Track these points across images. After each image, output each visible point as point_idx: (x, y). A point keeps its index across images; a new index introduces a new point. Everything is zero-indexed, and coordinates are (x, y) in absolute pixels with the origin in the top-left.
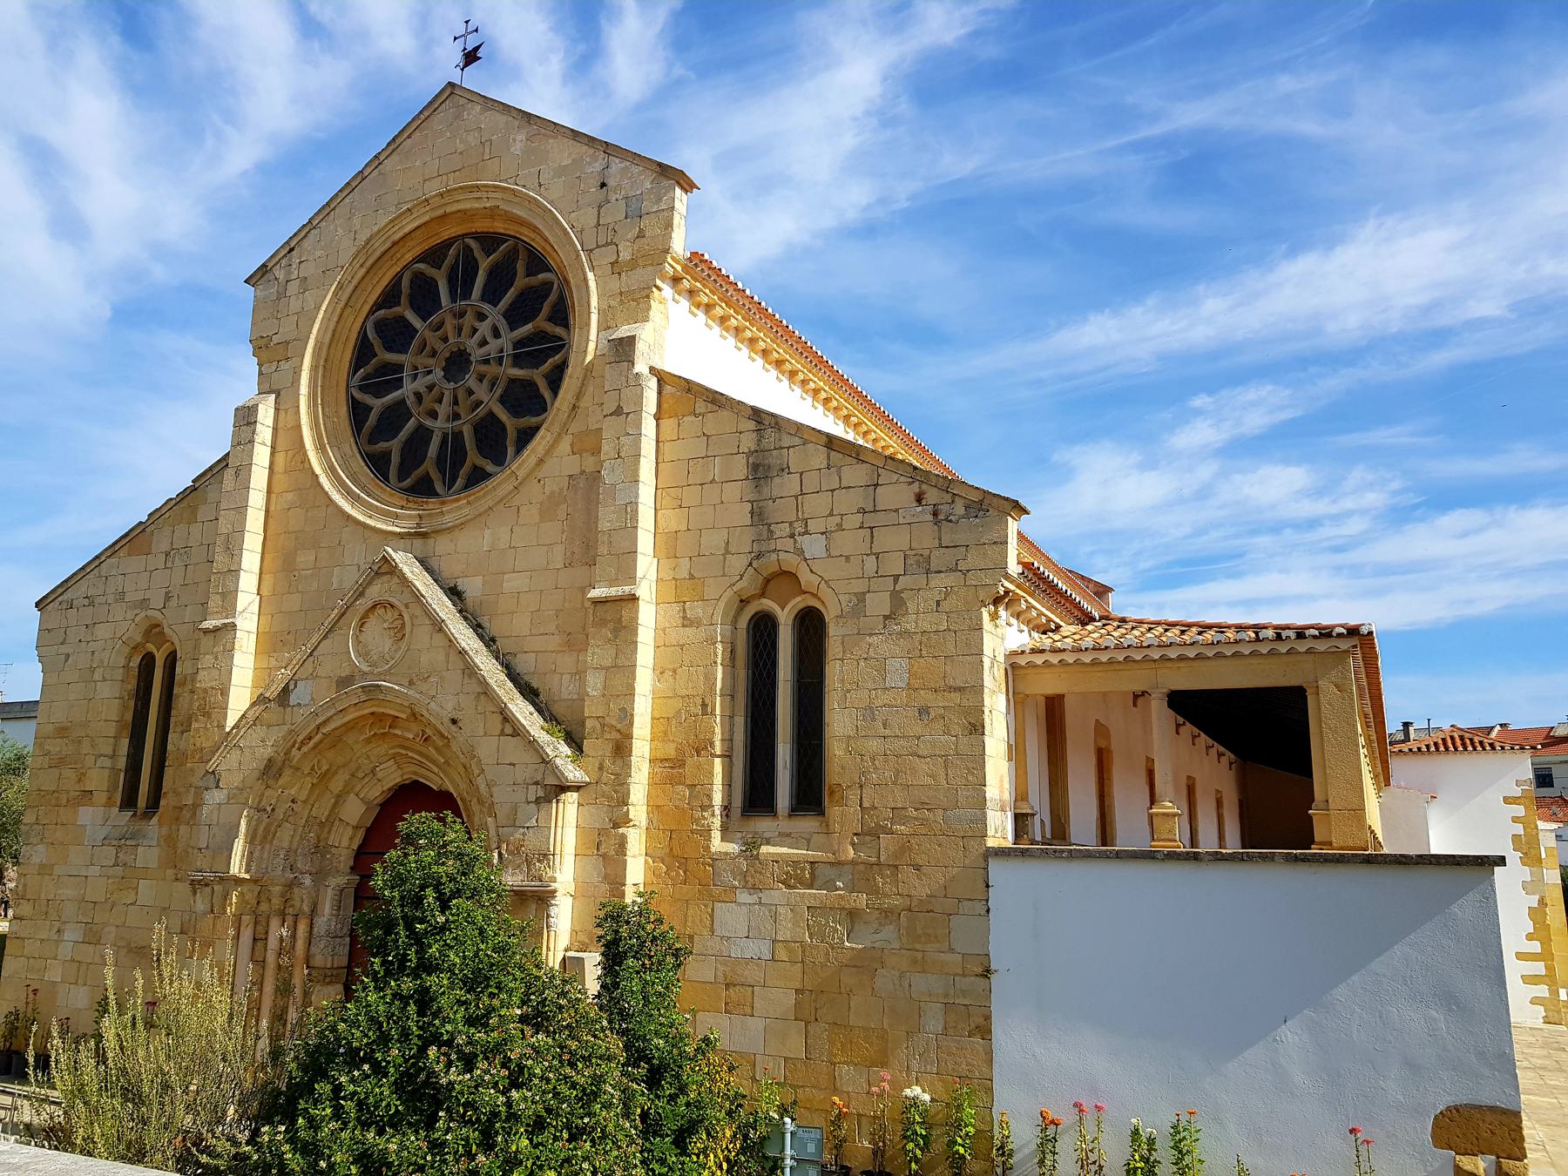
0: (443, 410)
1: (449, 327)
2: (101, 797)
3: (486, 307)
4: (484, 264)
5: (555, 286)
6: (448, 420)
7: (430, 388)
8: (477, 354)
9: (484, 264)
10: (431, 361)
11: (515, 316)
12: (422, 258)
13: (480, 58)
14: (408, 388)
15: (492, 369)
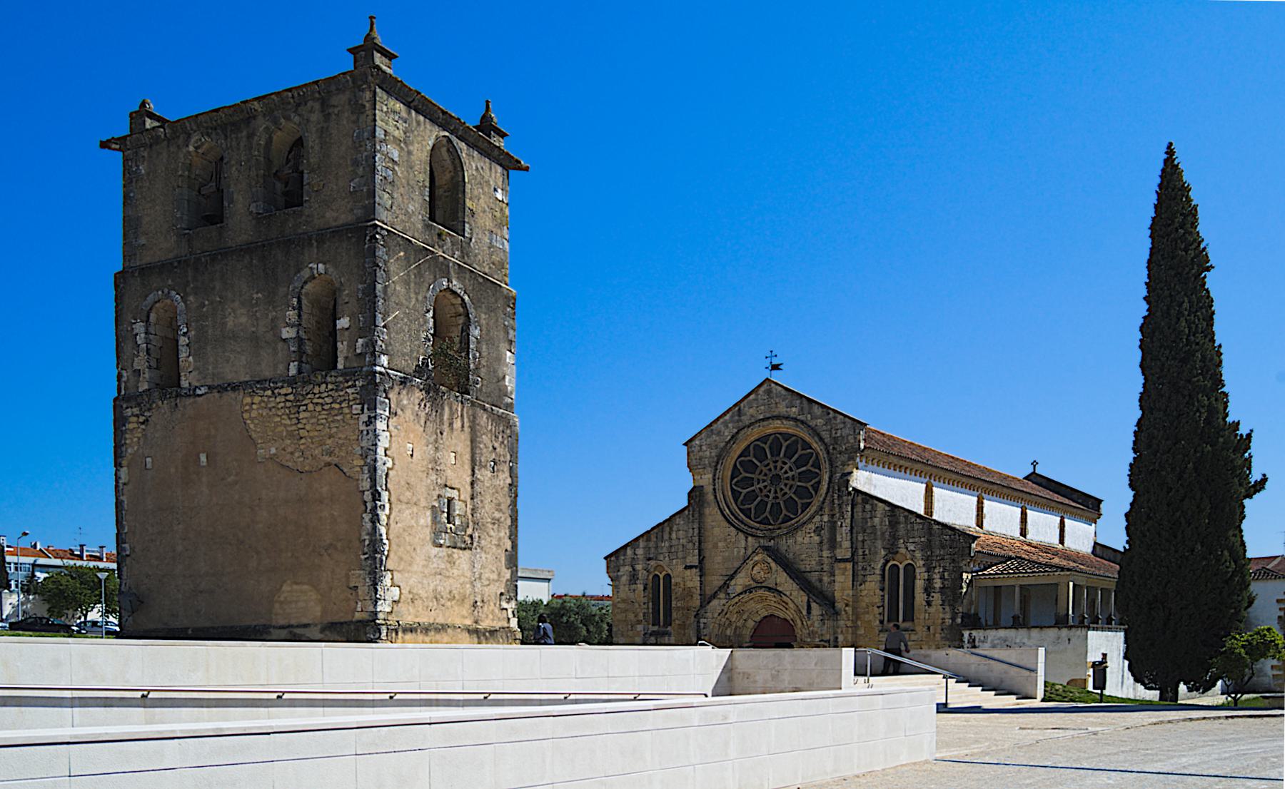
0: (772, 495)
4: (785, 444)
7: (765, 487)
9: (785, 444)
10: (765, 478)
11: (798, 464)
14: (756, 487)
15: (791, 482)
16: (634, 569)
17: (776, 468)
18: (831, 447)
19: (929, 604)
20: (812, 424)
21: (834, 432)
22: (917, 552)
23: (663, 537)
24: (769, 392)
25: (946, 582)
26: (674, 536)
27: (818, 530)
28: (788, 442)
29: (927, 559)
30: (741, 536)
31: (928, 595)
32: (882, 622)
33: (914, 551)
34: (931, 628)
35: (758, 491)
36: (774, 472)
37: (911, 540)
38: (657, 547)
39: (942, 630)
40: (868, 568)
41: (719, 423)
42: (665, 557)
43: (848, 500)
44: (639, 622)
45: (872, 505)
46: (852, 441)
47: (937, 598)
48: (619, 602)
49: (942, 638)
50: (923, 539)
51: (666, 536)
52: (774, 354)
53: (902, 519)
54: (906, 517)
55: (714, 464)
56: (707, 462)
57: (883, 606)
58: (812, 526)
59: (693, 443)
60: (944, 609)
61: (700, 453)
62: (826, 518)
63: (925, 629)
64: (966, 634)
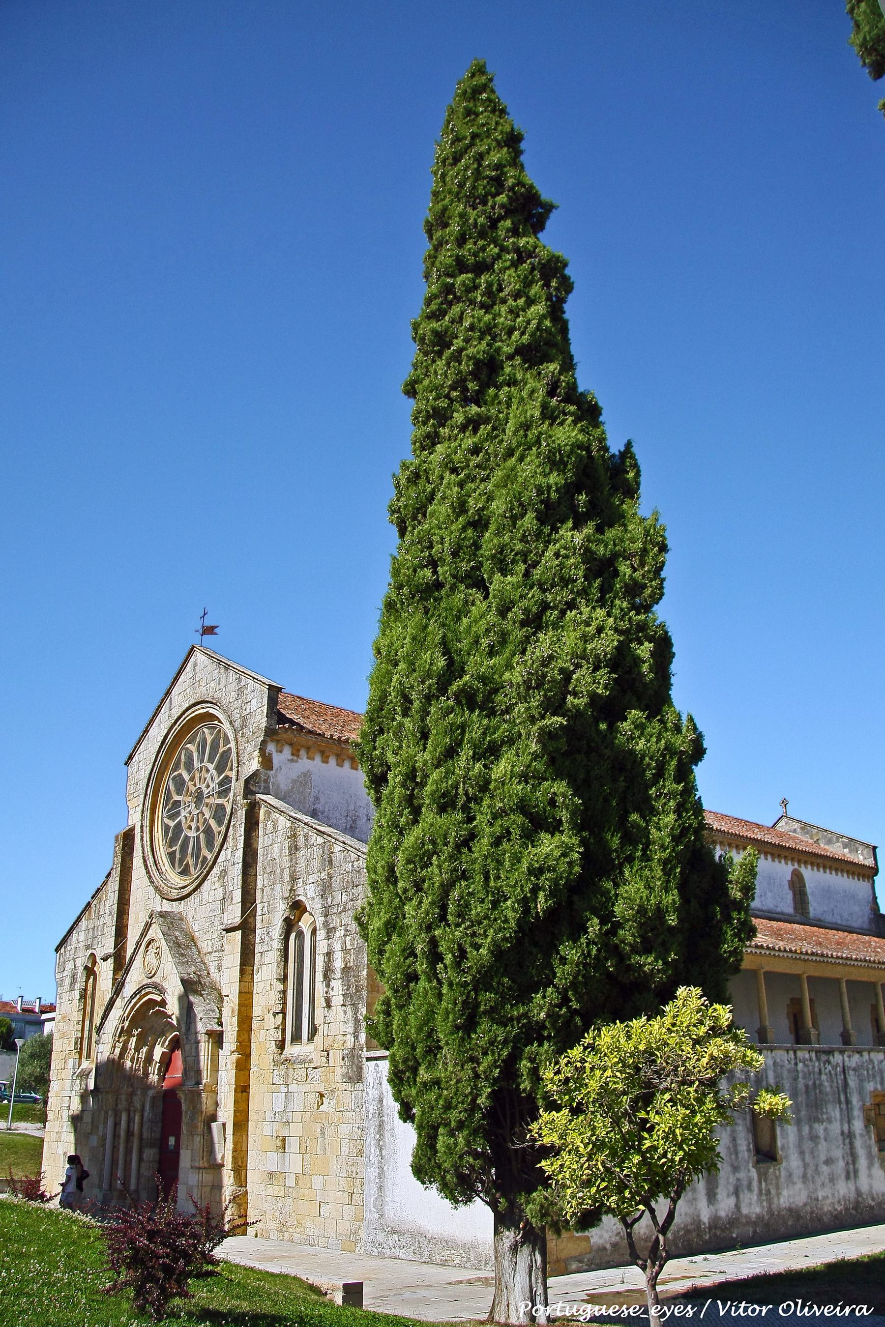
22: (317, 900)
31: (328, 986)
32: (281, 1046)
33: (313, 899)
39: (343, 1059)
40: (266, 939)
49: (343, 1076)
57: (283, 1012)
60: (345, 1012)
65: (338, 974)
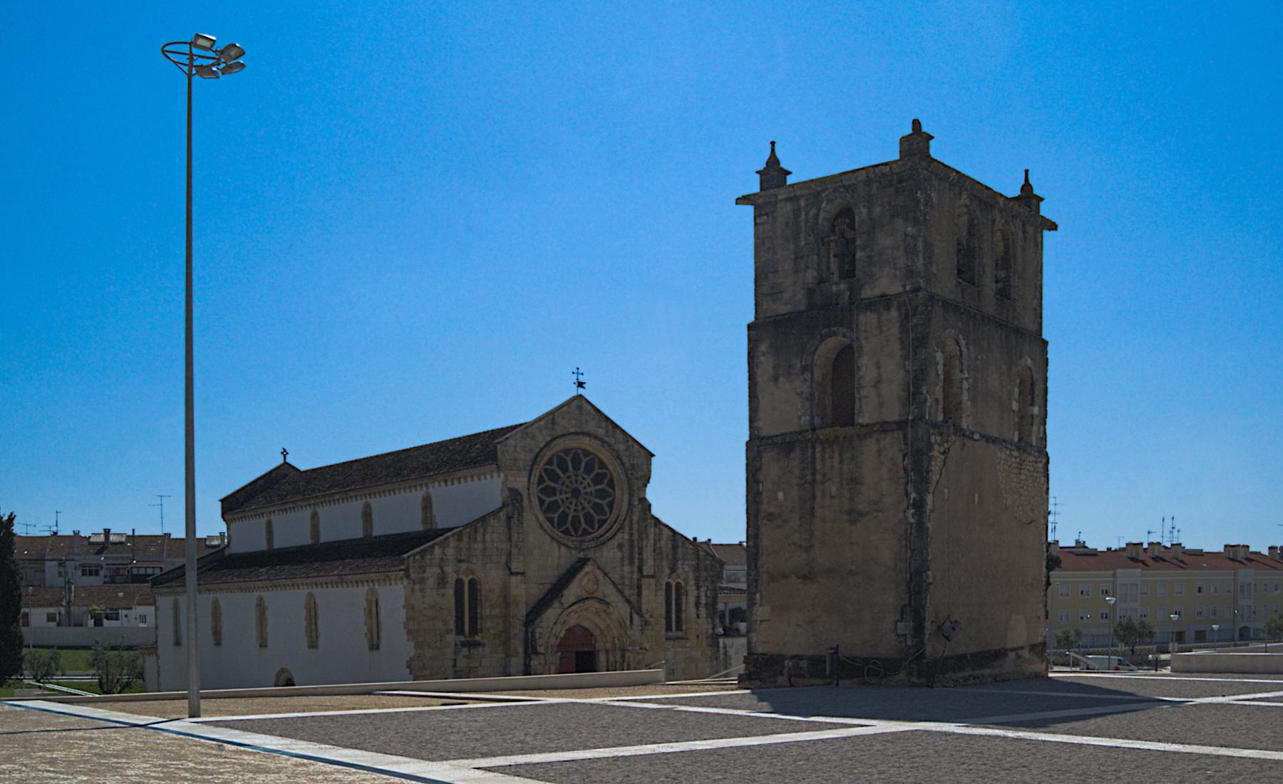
0: (573, 507)
1: (573, 478)
2: (454, 632)
3: (586, 476)
5: (608, 476)
6: (575, 510)
8: (583, 491)
12: (561, 451)
13: (584, 388)
16: (443, 572)
17: (576, 481)
18: (630, 472)
19: (698, 616)
20: (616, 447)
21: (632, 459)
23: (476, 538)
24: (580, 408)
25: (709, 599)
26: (488, 538)
27: (620, 546)
28: (588, 459)
29: (697, 579)
30: (555, 545)
31: (698, 609)
33: (688, 572)
34: (700, 636)
35: (560, 502)
36: (575, 485)
37: (686, 563)
38: (470, 548)
41: (534, 426)
42: (478, 561)
43: (651, 524)
44: (449, 631)
45: (660, 529)
46: (645, 470)
47: (703, 611)
48: (425, 608)
50: (694, 563)
51: (480, 538)
52: (575, 371)
53: (680, 544)
54: (683, 543)
55: (528, 468)
56: (521, 465)
58: (615, 542)
59: (508, 442)
61: (515, 454)
62: (626, 537)
63: (695, 637)
64: (721, 641)
65: (703, 605)
